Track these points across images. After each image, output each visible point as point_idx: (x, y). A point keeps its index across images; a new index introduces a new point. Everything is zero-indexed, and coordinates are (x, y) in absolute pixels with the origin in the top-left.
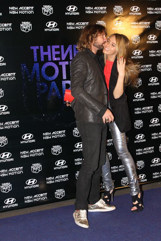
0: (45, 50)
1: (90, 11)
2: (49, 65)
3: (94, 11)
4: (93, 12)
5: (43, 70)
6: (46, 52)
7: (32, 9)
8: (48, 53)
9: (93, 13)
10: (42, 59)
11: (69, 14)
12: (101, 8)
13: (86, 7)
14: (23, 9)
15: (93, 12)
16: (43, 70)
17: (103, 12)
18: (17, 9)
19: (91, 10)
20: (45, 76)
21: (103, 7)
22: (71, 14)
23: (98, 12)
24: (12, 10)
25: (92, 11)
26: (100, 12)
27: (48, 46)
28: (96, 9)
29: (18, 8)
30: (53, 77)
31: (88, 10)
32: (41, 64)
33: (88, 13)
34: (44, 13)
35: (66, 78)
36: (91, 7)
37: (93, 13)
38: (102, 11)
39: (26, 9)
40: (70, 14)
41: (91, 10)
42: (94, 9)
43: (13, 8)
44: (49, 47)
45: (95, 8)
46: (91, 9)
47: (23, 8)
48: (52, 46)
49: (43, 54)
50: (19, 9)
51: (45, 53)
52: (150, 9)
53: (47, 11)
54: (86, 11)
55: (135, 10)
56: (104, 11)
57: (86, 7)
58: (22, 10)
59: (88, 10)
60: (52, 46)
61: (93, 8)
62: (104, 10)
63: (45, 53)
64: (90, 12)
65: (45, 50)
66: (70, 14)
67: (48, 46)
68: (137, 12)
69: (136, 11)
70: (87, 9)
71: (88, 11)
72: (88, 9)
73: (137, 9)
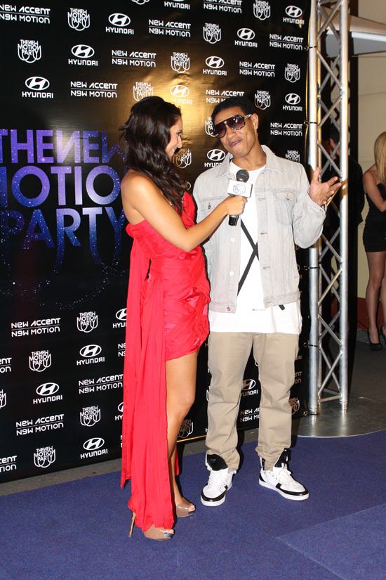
0: (22, 139)
2: (29, 173)
4: (88, 94)
5: (16, 182)
6: (22, 144)
8: (28, 146)
10: (15, 159)
11: (31, 95)
12: (106, 86)
13: (72, 83)
15: (88, 94)
16: (16, 182)
17: (109, 95)
19: (83, 90)
20: (19, 196)
21: (110, 84)
23: (97, 94)
26: (104, 94)
27: (28, 131)
28: (95, 88)
30: (36, 199)
31: (75, 89)
32: (12, 169)
33: (75, 94)
35: (64, 204)
36: (84, 83)
38: (107, 92)
40: (33, 96)
44: (30, 133)
45: (93, 84)
48: (38, 131)
49: (16, 146)
51: (22, 146)
52: (244, 64)
54: (72, 92)
55: (215, 65)
56: (111, 92)
57: (72, 83)
59: (75, 89)
60: (38, 131)
61: (88, 86)
62: (111, 90)
63: (22, 146)
64: (80, 94)
65: (22, 139)
66: (33, 96)
67: (28, 131)
68: (218, 69)
69: (217, 67)
73: (218, 62)
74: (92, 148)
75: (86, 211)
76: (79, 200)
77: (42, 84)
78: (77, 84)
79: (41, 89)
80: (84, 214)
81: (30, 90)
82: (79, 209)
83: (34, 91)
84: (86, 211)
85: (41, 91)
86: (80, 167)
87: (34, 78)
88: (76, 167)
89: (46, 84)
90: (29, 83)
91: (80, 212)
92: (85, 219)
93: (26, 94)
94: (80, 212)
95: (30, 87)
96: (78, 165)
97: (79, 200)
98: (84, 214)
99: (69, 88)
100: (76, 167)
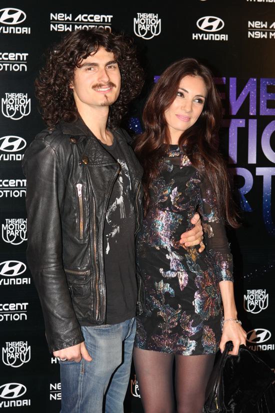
1: (260, 31)
3: (271, 34)
4: (268, 35)
7: (108, 22)
9: (266, 37)
11: (203, 37)
13: (249, 23)
14: (86, 20)
15: (268, 35)
18: (70, 19)
22: (208, 37)
24: (58, 20)
25: (264, 33)
29: (73, 18)
31: (253, 30)
33: (253, 36)
34: (139, 34)
37: (266, 37)
39: (92, 21)
40: (205, 39)
41: (263, 30)
42: (271, 27)
43: (60, 16)
46: (262, 27)
47: (85, 18)
50: (76, 20)
53: (147, 29)
54: (249, 33)
57: (249, 23)
58: (82, 23)
59: (253, 30)
64: (259, 35)
66: (205, 39)
70: (253, 26)
71: (255, 31)
72: (255, 28)
74: (270, 99)
75: (260, 171)
76: (252, 159)
77: (215, 24)
78: (256, 24)
79: (214, 30)
80: (257, 174)
81: (201, 32)
82: (252, 168)
83: (206, 33)
84: (260, 171)
85: (214, 33)
86: (256, 120)
87: (207, 18)
88: (250, 121)
89: (220, 24)
90: (200, 24)
91: (253, 172)
92: (259, 180)
93: (197, 37)
94: (253, 172)
95: (202, 28)
96: (253, 117)
97: (252, 159)
98: (257, 174)
99: (247, 29)
100: (250, 121)
